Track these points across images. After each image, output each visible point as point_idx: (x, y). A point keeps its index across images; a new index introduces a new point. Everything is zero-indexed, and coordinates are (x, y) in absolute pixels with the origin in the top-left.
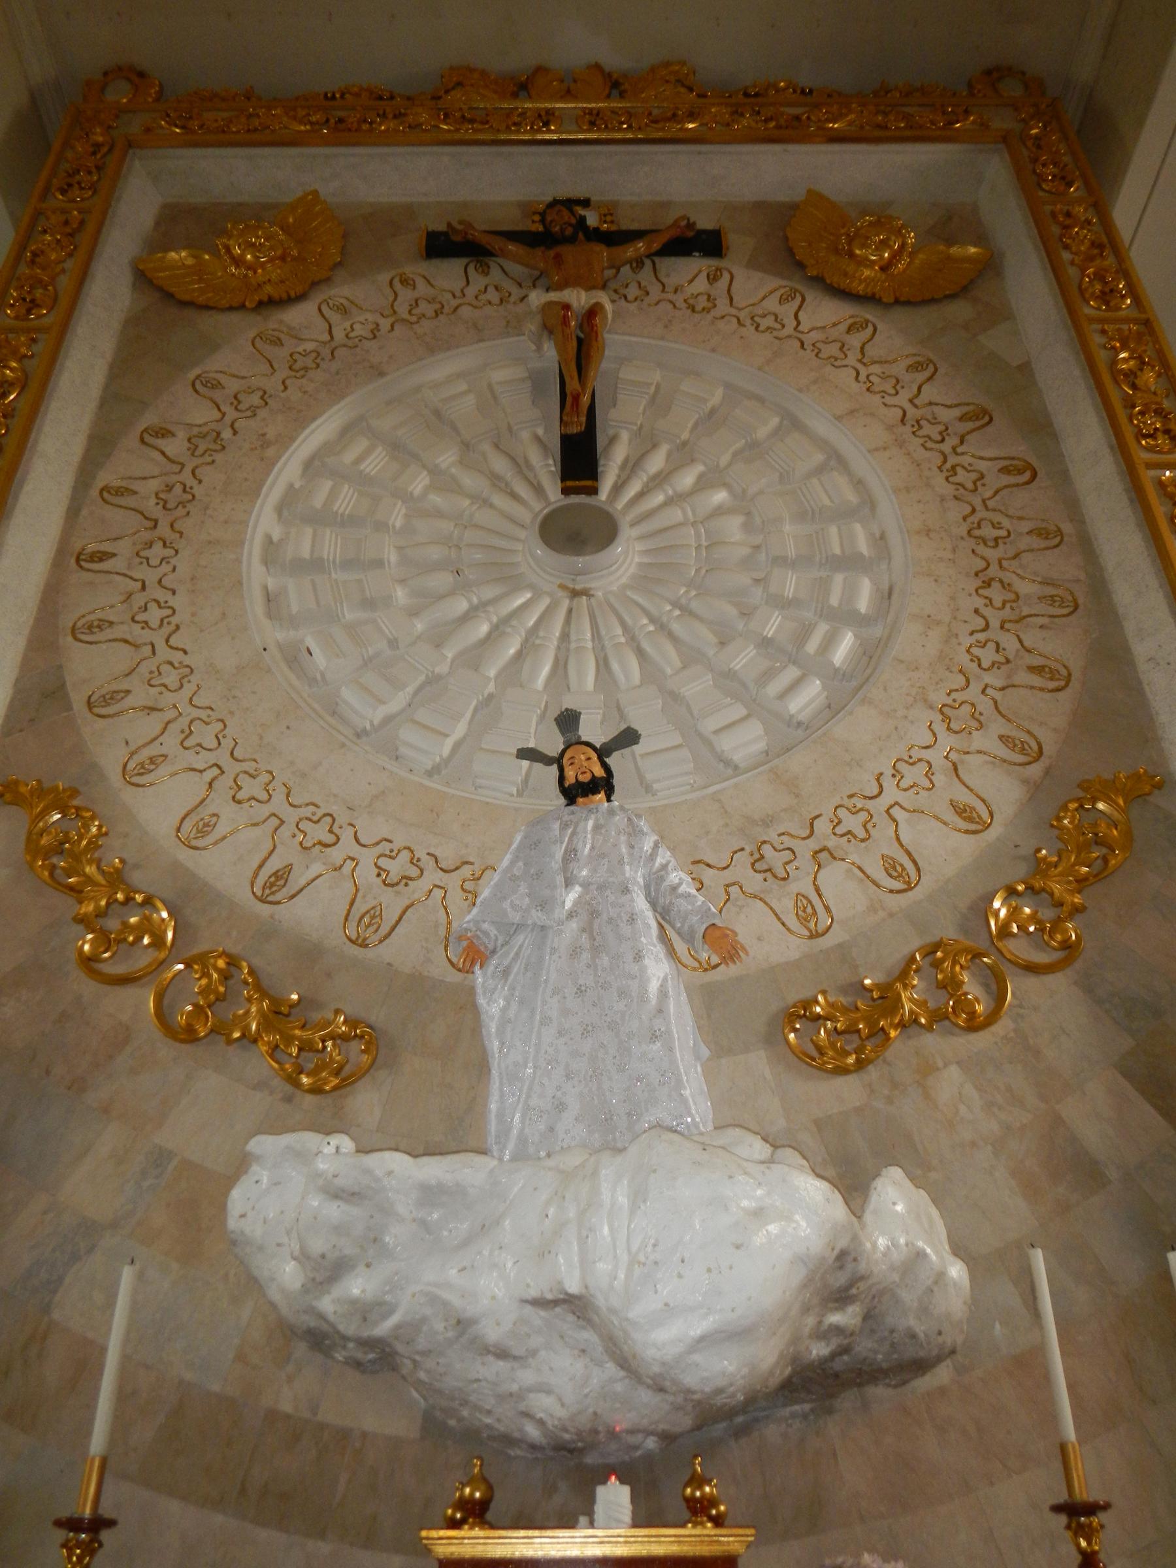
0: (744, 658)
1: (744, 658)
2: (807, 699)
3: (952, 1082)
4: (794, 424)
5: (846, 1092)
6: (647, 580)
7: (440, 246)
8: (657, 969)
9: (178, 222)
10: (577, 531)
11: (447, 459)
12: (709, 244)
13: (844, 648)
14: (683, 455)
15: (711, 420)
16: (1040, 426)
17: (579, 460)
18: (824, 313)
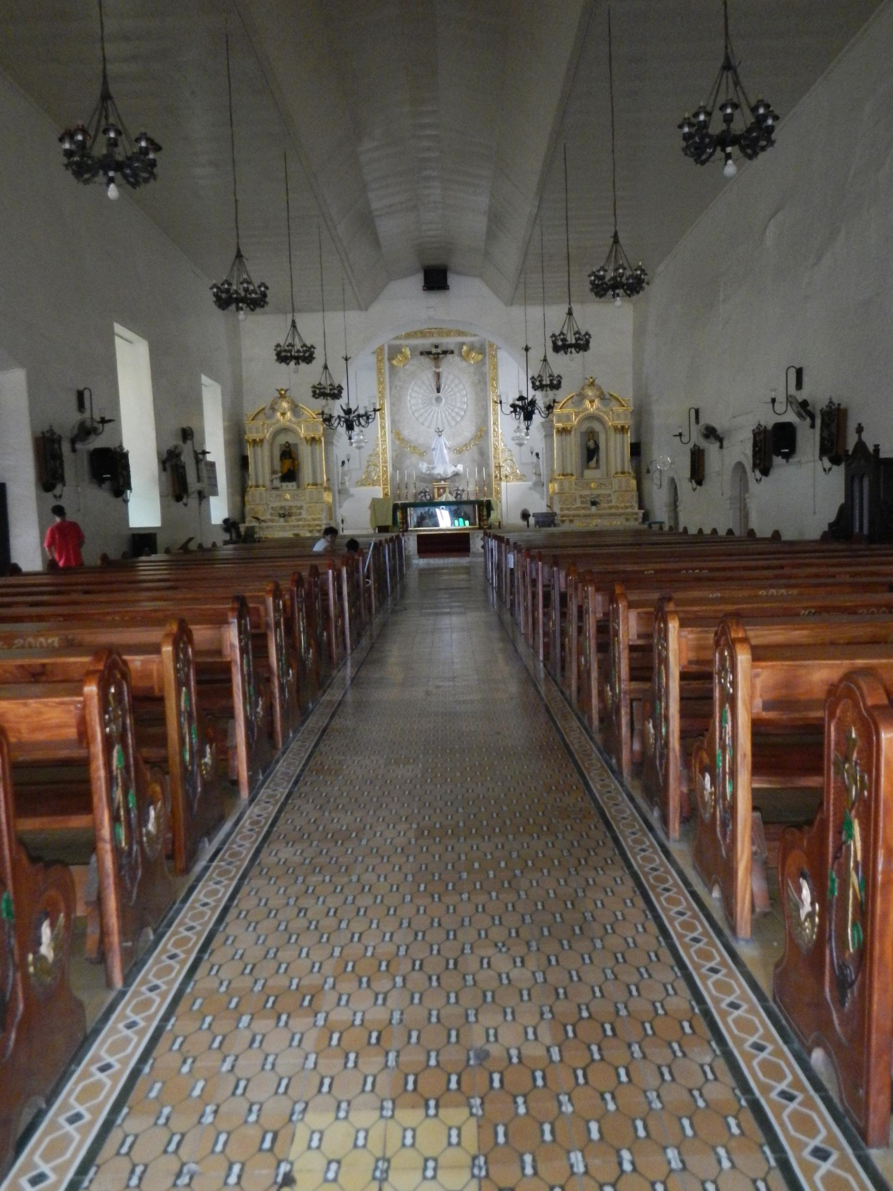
0: (454, 414)
1: (454, 414)
2: (459, 419)
3: (467, 455)
4: (460, 382)
5: (458, 456)
6: (445, 404)
7: (422, 354)
8: (445, 451)
9: (390, 347)
10: (438, 400)
11: (425, 388)
12: (452, 352)
13: (463, 413)
14: (449, 387)
15: (452, 381)
16: (485, 383)
17: (438, 391)
18: (464, 364)
